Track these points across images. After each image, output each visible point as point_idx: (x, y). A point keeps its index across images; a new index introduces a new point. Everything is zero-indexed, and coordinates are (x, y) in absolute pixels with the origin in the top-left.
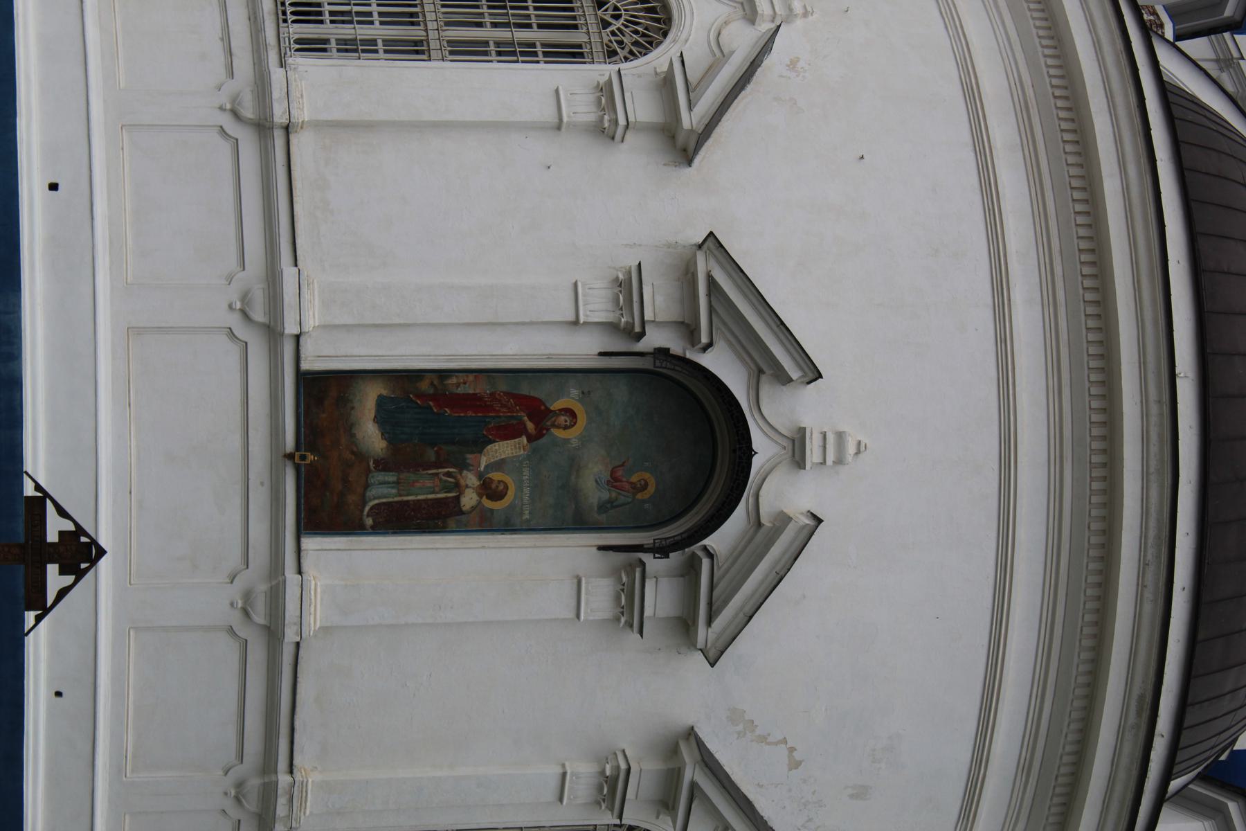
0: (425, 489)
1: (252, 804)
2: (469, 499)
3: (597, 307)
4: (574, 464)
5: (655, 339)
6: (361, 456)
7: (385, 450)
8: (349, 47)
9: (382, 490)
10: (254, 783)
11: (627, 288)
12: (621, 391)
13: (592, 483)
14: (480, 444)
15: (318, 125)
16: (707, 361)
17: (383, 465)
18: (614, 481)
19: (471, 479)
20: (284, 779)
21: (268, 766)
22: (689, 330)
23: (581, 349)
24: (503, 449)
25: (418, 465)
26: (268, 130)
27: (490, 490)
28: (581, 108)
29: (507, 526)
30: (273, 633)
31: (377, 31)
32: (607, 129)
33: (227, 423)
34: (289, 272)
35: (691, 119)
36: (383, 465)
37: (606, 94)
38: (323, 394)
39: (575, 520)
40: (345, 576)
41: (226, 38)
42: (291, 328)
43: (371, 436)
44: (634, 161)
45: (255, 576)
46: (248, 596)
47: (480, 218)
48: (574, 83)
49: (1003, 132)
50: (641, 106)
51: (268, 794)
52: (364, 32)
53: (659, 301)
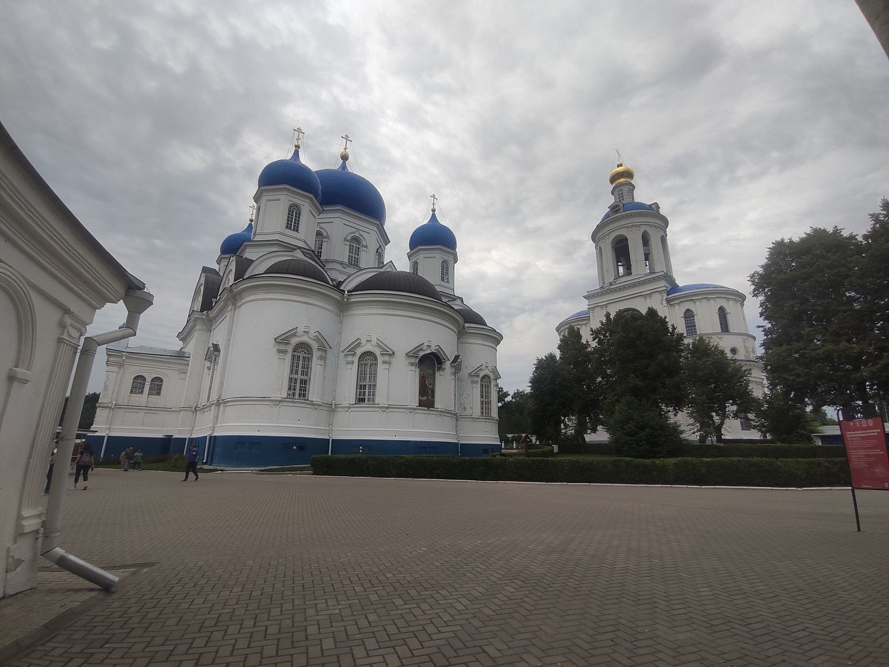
3: (414, 368)
9: (430, 398)
11: (412, 364)
13: (431, 372)
23: (418, 370)
32: (390, 363)
33: (423, 416)
37: (384, 362)
40: (438, 404)
43: (425, 398)
44: (393, 360)
47: (399, 382)
48: (381, 367)
49: (391, 312)
50: (387, 358)
53: (413, 360)
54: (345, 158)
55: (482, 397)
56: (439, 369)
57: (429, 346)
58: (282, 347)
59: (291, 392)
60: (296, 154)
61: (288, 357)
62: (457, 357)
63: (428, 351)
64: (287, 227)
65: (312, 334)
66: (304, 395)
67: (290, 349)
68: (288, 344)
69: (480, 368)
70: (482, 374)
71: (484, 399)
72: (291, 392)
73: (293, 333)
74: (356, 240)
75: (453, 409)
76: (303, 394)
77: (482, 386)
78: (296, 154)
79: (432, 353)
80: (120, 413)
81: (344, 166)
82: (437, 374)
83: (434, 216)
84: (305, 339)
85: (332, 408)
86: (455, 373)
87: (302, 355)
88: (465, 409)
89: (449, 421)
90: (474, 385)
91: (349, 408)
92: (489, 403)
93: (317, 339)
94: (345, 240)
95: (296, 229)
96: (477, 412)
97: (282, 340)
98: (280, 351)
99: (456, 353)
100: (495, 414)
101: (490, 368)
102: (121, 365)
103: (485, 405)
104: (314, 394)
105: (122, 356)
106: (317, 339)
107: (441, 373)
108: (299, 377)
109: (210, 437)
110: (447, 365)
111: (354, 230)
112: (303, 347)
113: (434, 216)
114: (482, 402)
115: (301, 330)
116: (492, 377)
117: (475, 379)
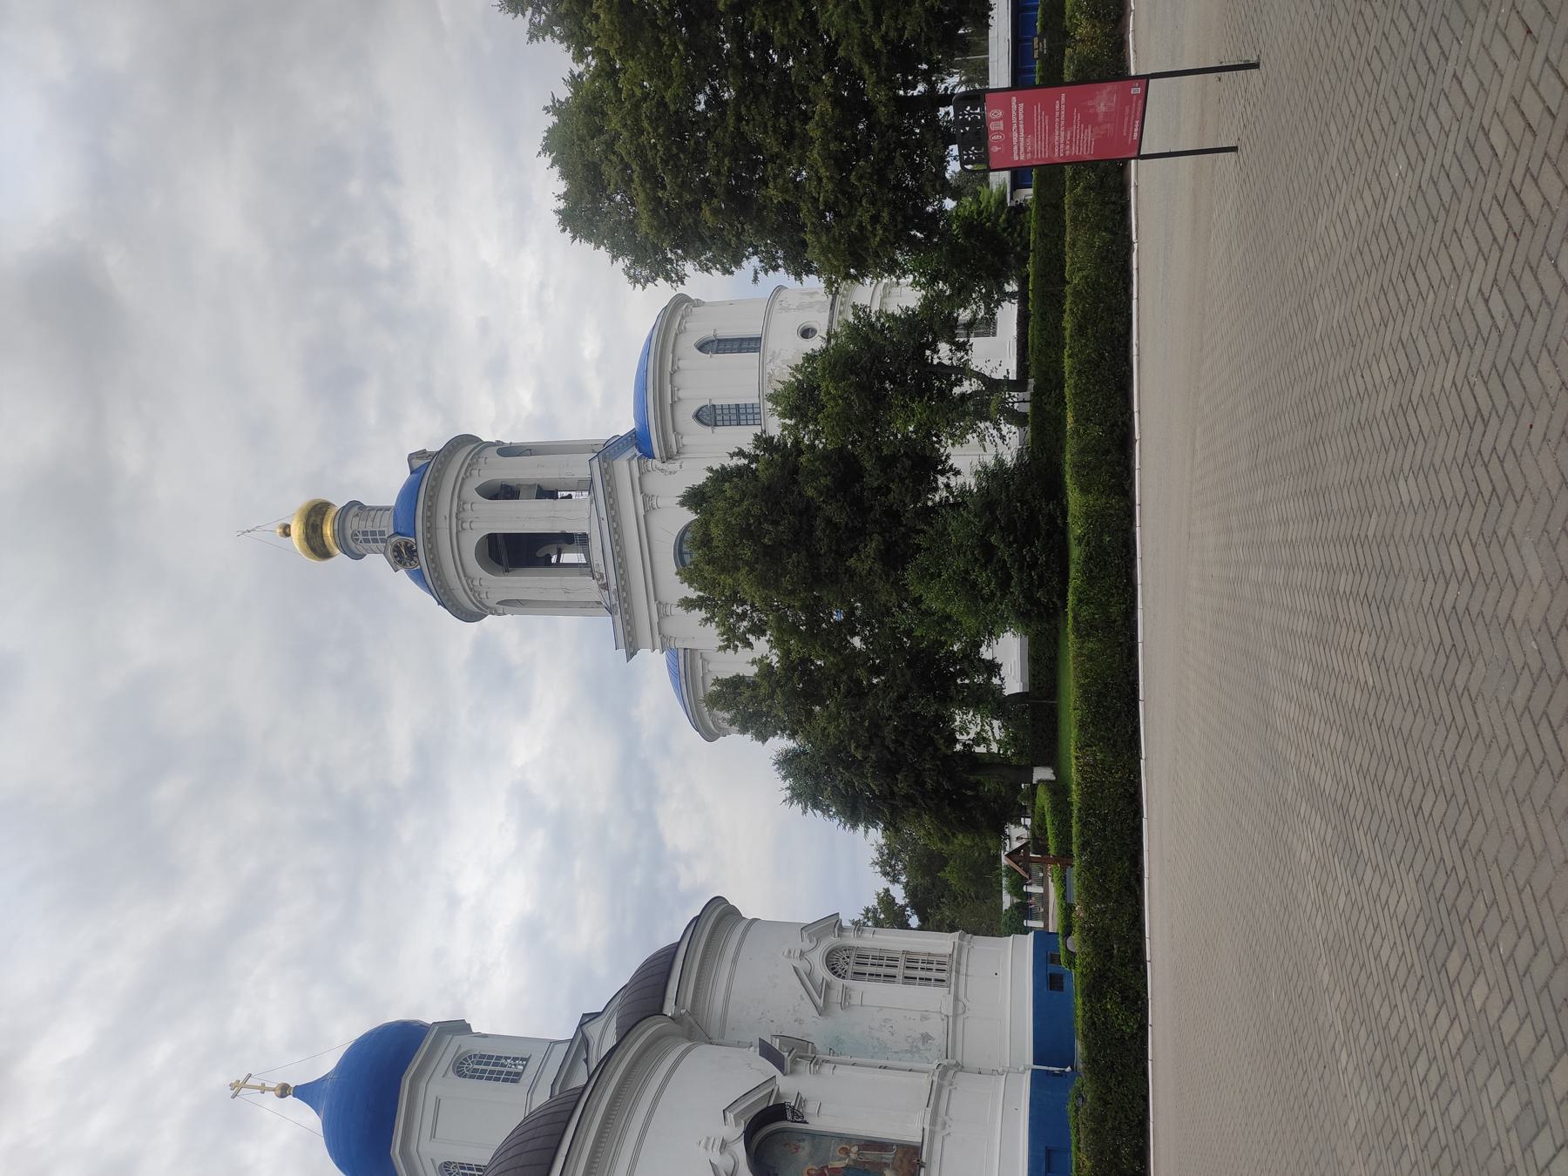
0: (871, 1155)
1: (940, 1120)
2: (855, 1149)
6: (895, 1169)
10: (938, 1128)
13: (806, 1148)
14: (847, 1168)
17: (887, 1165)
18: (797, 1149)
19: (853, 1156)
20: (927, 1128)
21: (940, 1087)
25: (872, 1163)
27: (847, 1152)
36: (887, 1165)
39: (817, 1136)
46: (944, 1127)
51: (933, 1122)
55: (890, 978)
56: (799, 1116)
57: (724, 1145)
62: (767, 1052)
63: (740, 1149)
69: (805, 977)
70: (822, 972)
75: (924, 1081)
77: (858, 975)
79: (749, 1134)
82: (816, 1123)
83: (304, 1093)
86: (816, 1061)
88: (926, 1038)
89: (965, 1096)
90: (855, 1000)
92: (911, 960)
96: (933, 998)
99: (754, 1052)
100: (940, 943)
101: (807, 945)
103: (918, 971)
107: (810, 1109)
110: (789, 1087)
113: (304, 1093)
114: (909, 979)
116: (832, 941)
117: (836, 995)
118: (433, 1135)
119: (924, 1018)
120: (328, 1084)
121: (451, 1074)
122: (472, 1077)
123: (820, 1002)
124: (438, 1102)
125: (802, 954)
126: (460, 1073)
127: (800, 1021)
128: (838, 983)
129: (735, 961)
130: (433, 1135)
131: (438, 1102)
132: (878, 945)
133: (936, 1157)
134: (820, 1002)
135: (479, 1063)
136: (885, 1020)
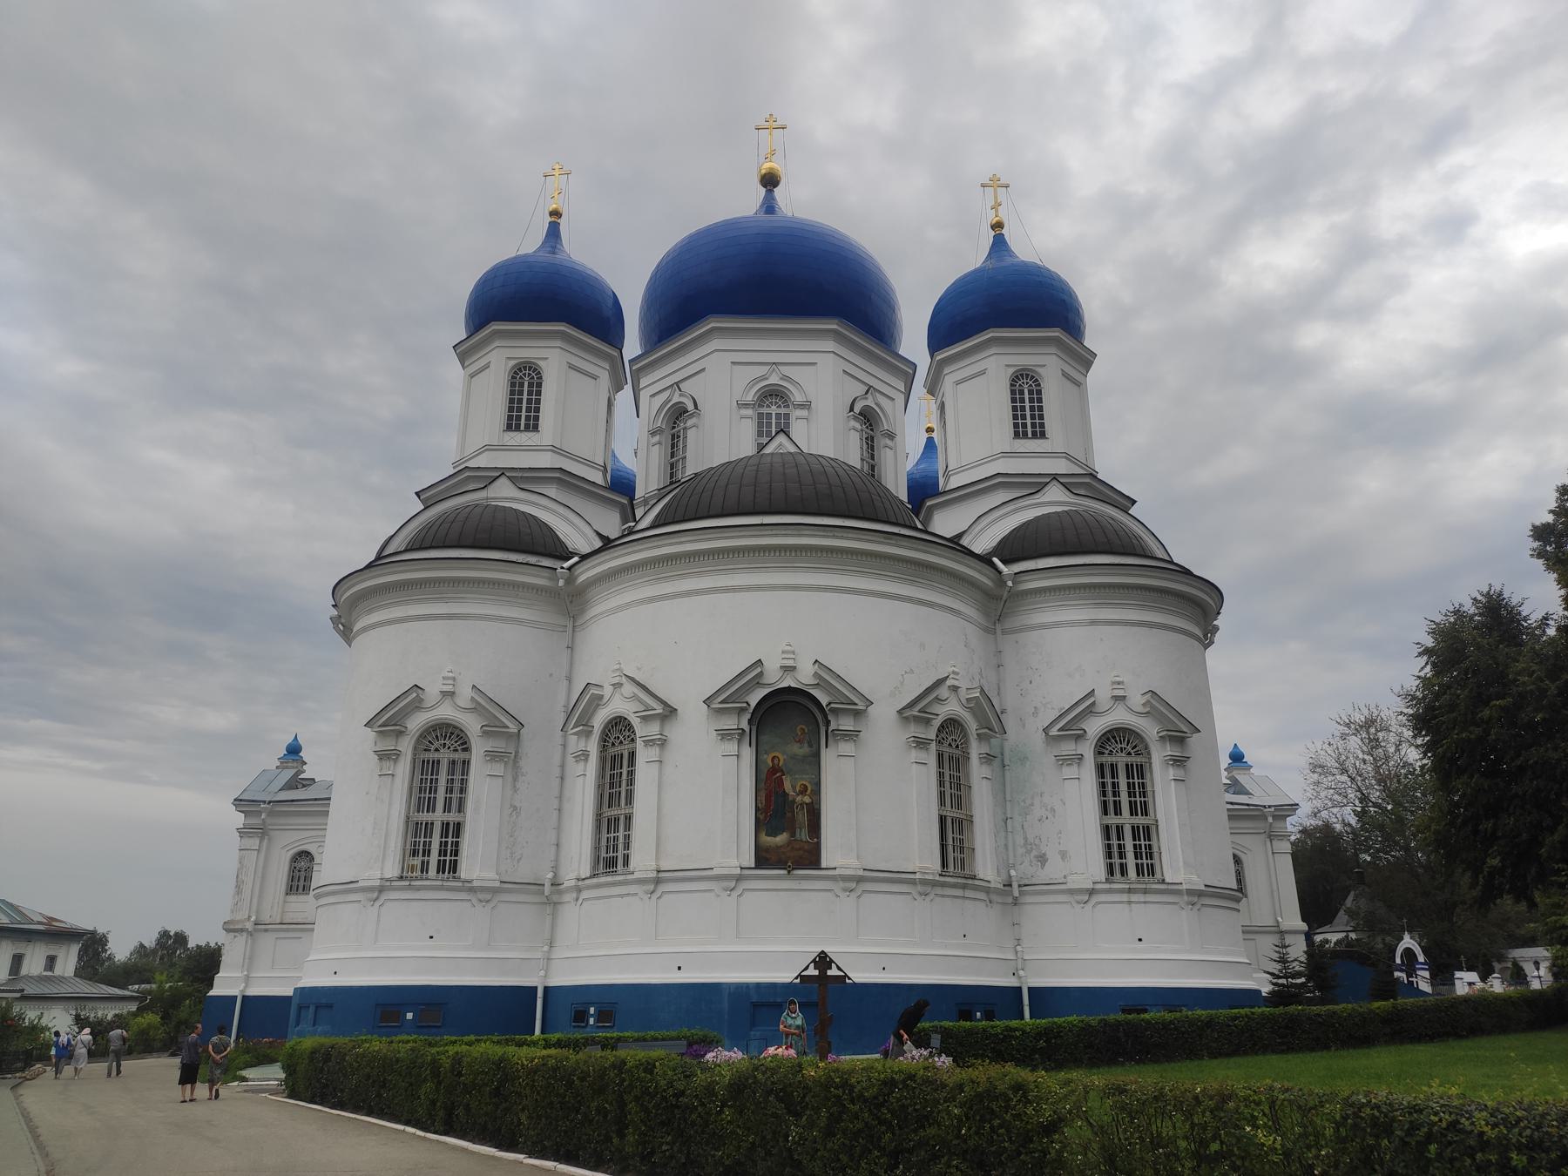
0: (802, 817)
1: (928, 889)
2: (807, 799)
3: (732, 747)
4: (794, 757)
5: (745, 725)
6: (789, 843)
7: (787, 831)
8: (627, 846)
9: (803, 835)
10: (920, 888)
11: (724, 735)
12: (764, 738)
13: (802, 750)
14: (785, 794)
15: (657, 859)
16: (753, 704)
17: (793, 834)
19: (799, 799)
20: (918, 876)
21: (913, 882)
22: (742, 710)
23: (748, 754)
24: (787, 786)
25: (793, 819)
26: (658, 879)
27: (804, 791)
28: (654, 753)
29: (818, 784)
30: (860, 880)
31: (621, 834)
32: (662, 743)
34: (715, 872)
35: (659, 710)
36: (793, 834)
37: (649, 743)
38: (764, 858)
39: (816, 756)
40: (836, 850)
41: (621, 896)
42: (738, 871)
43: (781, 839)
44: (675, 732)
45: (837, 887)
46: (845, 890)
47: (700, 793)
48: (644, 755)
50: (653, 729)
52: (621, 840)
53: (730, 723)
54: (770, 181)
58: (388, 745)
59: (417, 861)
60: (554, 232)
61: (403, 768)
64: (509, 428)
65: (465, 694)
66: (454, 867)
67: (406, 746)
68: (400, 734)
69: (1087, 707)
70: (1095, 727)
71: (1126, 819)
72: (417, 861)
73: (412, 699)
74: (773, 394)
76: (449, 865)
77: (1100, 769)
78: (554, 232)
80: (266, 941)
81: (769, 206)
82: (829, 757)
83: (999, 244)
84: (446, 712)
85: (548, 895)
87: (445, 756)
88: (1042, 859)
90: (1070, 771)
91: (381, 889)
93: (476, 709)
94: (742, 405)
95: (532, 426)
97: (388, 722)
98: (383, 756)
101: (1137, 700)
102: (262, 832)
104: (475, 863)
105: (260, 813)
106: (476, 709)
108: (438, 816)
109: (244, 997)
111: (764, 370)
112: (448, 733)
113: (999, 244)
115: (432, 690)
117: (1068, 748)
118: (958, 383)
119: (1063, 855)
120: (1008, 261)
121: (1012, 370)
122: (1013, 392)
123: (1054, 732)
124: (983, 372)
125: (1117, 698)
126: (1015, 380)
127: (1035, 714)
128: (1087, 750)
129: (1093, 622)
130: (958, 383)
131: (983, 372)
132: (1158, 788)
133: (806, 885)
134: (1054, 732)
135: (1031, 392)
136: (1053, 810)
